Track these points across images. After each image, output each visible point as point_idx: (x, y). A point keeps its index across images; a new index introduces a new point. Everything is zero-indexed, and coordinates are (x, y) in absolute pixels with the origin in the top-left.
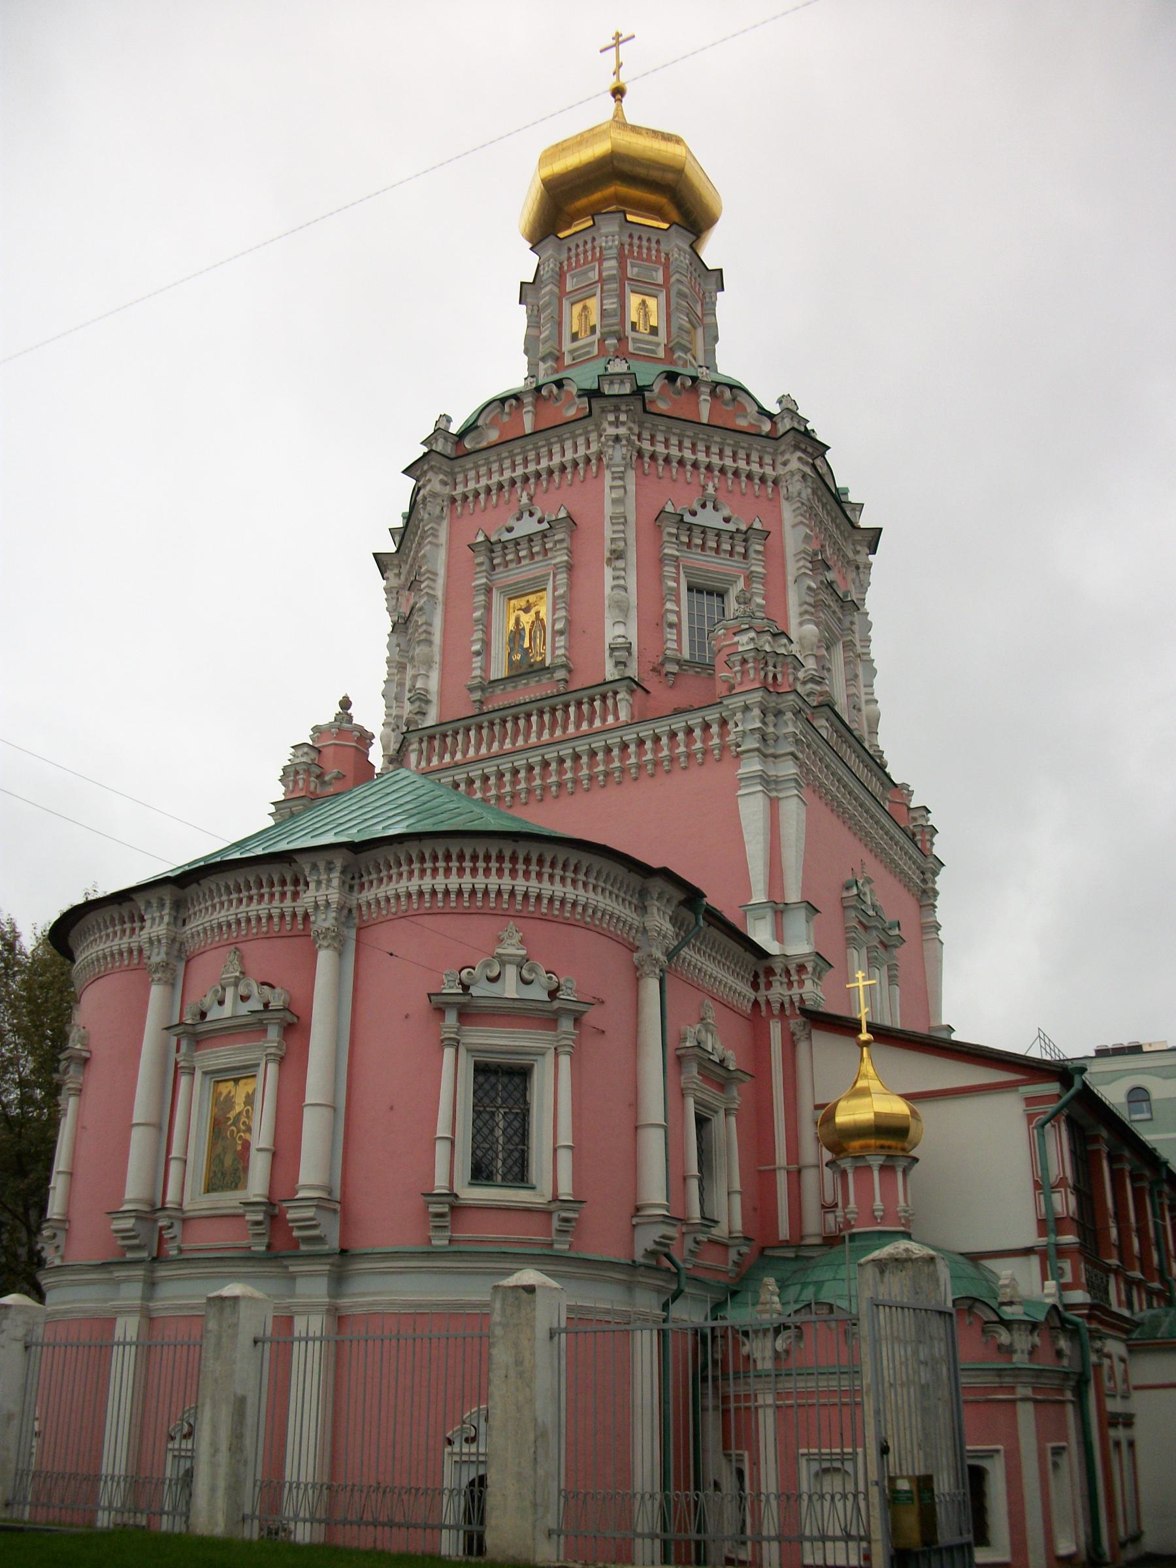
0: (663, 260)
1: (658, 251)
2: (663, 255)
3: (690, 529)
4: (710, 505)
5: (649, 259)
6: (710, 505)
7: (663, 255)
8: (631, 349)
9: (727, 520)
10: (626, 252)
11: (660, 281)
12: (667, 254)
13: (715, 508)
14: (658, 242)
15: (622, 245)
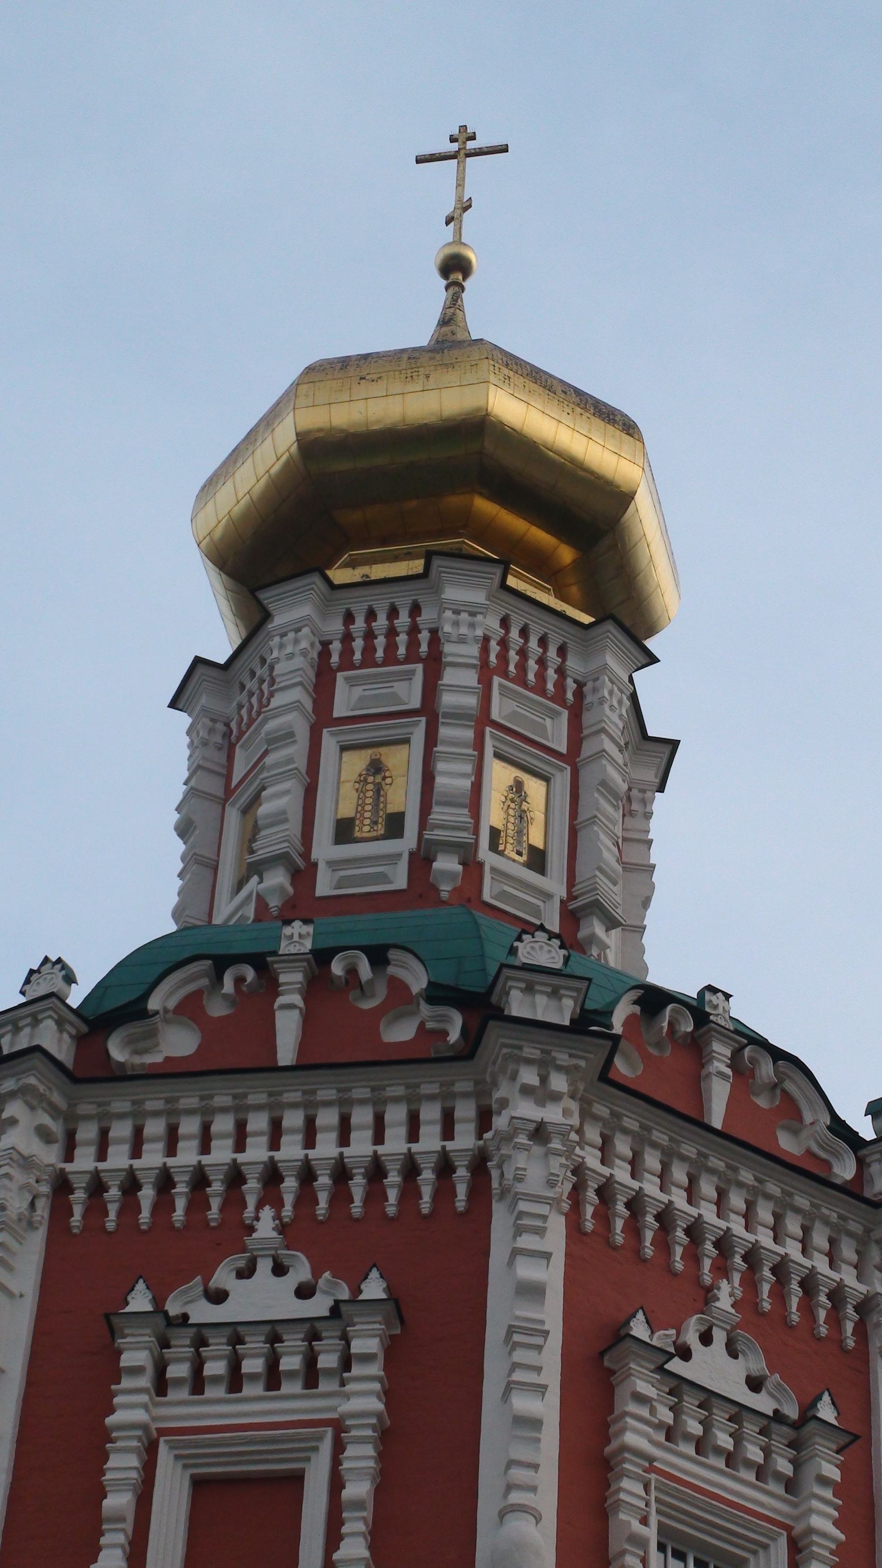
0: (424, 648)
1: (414, 630)
2: (424, 637)
3: (200, 1342)
4: (264, 1266)
5: (391, 658)
6: (264, 1266)
7: (424, 637)
8: (324, 886)
9: (304, 1292)
10: (335, 659)
11: (415, 702)
12: (434, 633)
13: (279, 1270)
14: (415, 610)
15: (326, 645)
